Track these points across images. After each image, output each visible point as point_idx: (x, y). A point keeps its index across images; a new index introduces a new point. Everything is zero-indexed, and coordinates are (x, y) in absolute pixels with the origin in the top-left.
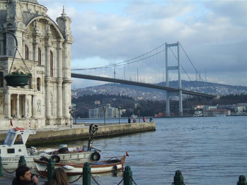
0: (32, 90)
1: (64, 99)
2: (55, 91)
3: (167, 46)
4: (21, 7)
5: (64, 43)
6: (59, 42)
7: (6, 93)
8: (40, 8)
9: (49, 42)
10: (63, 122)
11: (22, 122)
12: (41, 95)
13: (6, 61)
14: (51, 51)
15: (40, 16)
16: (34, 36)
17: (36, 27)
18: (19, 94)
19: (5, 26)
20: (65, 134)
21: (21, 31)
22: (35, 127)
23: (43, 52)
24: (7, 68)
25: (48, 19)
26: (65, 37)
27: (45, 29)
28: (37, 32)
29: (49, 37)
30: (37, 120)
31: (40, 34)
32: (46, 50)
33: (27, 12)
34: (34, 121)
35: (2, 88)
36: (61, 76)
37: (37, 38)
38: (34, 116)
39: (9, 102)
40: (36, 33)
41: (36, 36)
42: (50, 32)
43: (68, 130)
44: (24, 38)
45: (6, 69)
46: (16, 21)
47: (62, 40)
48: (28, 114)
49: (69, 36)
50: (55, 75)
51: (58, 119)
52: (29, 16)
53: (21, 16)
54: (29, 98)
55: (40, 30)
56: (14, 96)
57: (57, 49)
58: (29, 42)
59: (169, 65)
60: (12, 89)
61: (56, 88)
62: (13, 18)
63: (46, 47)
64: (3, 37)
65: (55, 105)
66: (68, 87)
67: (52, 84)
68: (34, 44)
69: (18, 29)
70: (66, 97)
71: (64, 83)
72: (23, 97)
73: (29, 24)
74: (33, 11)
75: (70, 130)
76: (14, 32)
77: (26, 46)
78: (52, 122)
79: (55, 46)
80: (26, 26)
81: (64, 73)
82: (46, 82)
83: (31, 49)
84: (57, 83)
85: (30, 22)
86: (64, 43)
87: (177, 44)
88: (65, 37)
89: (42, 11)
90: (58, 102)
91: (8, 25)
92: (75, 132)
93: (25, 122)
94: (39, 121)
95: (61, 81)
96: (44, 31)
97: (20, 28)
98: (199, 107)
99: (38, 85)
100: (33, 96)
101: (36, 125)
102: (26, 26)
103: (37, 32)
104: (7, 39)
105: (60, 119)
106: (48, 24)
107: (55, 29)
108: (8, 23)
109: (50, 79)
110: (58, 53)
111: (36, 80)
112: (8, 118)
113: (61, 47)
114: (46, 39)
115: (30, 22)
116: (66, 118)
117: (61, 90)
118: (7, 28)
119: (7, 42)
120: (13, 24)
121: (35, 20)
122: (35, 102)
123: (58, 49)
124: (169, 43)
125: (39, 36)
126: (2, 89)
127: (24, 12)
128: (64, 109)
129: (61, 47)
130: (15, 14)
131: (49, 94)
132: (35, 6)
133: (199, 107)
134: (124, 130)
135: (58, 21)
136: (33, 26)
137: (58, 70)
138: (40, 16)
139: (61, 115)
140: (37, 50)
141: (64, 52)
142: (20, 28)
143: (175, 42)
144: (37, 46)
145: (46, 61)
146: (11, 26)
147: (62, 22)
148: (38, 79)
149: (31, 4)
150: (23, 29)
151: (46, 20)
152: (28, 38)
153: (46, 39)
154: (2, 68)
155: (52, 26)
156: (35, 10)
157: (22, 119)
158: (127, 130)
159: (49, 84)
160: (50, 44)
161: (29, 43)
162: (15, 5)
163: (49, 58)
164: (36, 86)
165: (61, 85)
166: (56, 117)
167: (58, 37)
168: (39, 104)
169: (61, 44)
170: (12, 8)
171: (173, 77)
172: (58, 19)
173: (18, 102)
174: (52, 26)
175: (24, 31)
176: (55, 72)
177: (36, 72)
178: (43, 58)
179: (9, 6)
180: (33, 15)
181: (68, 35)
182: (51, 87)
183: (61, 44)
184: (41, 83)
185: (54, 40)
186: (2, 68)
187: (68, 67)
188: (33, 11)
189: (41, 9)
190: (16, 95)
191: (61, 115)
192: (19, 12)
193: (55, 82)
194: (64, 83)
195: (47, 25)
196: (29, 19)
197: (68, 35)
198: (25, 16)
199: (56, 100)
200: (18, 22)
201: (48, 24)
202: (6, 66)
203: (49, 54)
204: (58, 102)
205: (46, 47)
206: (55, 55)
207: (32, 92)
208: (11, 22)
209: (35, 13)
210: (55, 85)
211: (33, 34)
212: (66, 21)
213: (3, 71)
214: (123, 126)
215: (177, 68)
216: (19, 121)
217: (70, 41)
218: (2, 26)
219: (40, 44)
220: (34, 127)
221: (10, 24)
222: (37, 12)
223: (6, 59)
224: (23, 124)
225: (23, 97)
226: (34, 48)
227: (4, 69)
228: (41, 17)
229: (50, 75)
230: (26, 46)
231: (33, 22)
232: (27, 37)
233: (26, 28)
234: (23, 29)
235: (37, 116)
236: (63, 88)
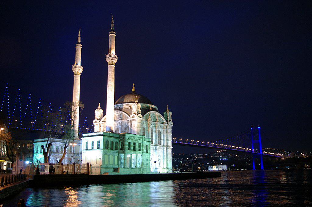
2: (162, 153)
14: (159, 131)
50: (162, 144)
164: (145, 150)
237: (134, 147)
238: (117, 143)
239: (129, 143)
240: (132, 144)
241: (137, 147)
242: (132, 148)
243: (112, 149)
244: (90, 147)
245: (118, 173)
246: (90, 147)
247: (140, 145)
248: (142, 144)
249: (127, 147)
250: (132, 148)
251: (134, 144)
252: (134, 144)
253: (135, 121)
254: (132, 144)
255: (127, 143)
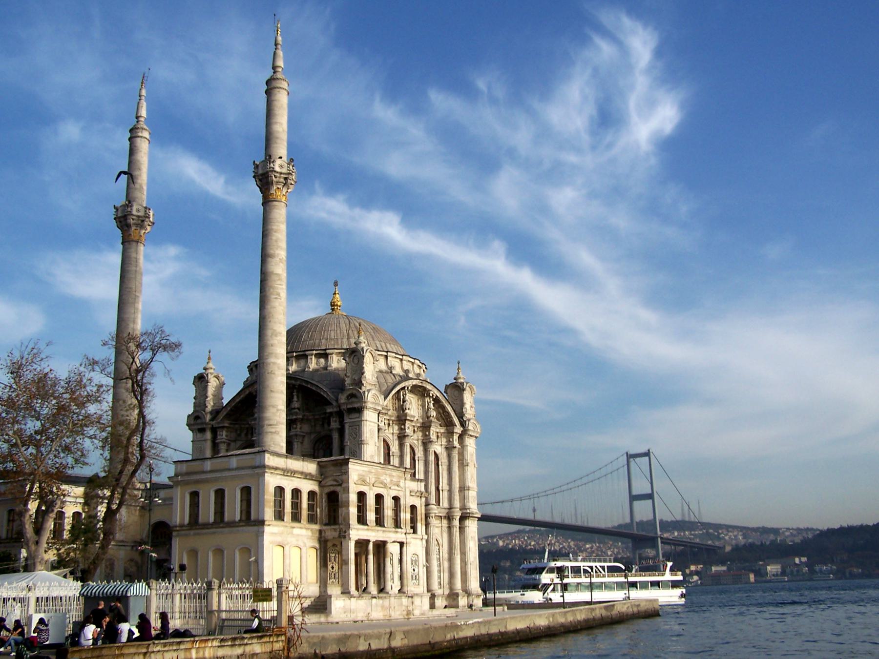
0: (400, 530)
1: (463, 553)
2: (445, 535)
3: (630, 457)
4: (375, 360)
5: (461, 437)
6: (450, 433)
7: (345, 537)
8: (413, 364)
9: (431, 432)
10: (463, 601)
11: (381, 601)
12: (419, 542)
13: (344, 467)
15: (412, 379)
16: (401, 419)
17: (404, 401)
18: (373, 539)
19: (343, 399)
20: (484, 631)
21: (376, 410)
22: (408, 614)
23: (420, 453)
24: (348, 482)
25: (429, 387)
26: (463, 424)
27: (423, 406)
28: (407, 411)
29: (431, 422)
30: (412, 597)
31: (414, 417)
32: (426, 451)
33: (386, 372)
34: (405, 601)
35: (336, 527)
36: (457, 504)
37: (408, 424)
38: (405, 589)
39: (352, 556)
40: (406, 415)
41: (406, 420)
42: (433, 413)
43: (488, 623)
44: (382, 425)
45: (344, 485)
46: (363, 389)
47: (458, 429)
48: (393, 585)
49: (472, 421)
51: (453, 596)
52: (390, 380)
53: (375, 379)
54: (393, 549)
55: (414, 408)
56: (362, 545)
57: (447, 448)
58: (391, 433)
59: (634, 493)
60: (358, 529)
61: (445, 529)
62: (359, 384)
63: (426, 443)
64: (338, 423)
65: (446, 564)
66: (472, 527)
67: (439, 521)
68: (402, 437)
69: (369, 405)
70: (467, 549)
71: (463, 518)
72: (381, 547)
73: (391, 395)
74: (398, 370)
75: (495, 620)
76: (359, 411)
77: (384, 440)
78: (440, 602)
79: (444, 441)
80: (385, 398)
81: (463, 499)
82: (427, 516)
83: (395, 448)
84: (449, 518)
85: (394, 392)
86: (461, 437)
87: (647, 454)
88: (463, 424)
89: (417, 370)
90: (451, 559)
91: (347, 397)
92: (506, 627)
93: (386, 602)
94: (417, 600)
95: (457, 514)
96: (421, 411)
97: (373, 403)
98: (693, 568)
99: (413, 521)
100: (402, 544)
101: (410, 608)
102: (385, 398)
103: (407, 411)
104: (347, 427)
105: (457, 595)
106: (428, 395)
107: (443, 407)
108: (349, 393)
109: (435, 510)
110: (449, 456)
111: (408, 510)
112: (349, 593)
113: (456, 444)
114: (425, 427)
115: (394, 392)
116: (468, 593)
117: (458, 533)
118: (347, 404)
119: (347, 431)
120: (358, 394)
121: (403, 388)
122: (407, 558)
123: (449, 448)
124: (632, 451)
125: (412, 421)
126: (335, 530)
127: (381, 371)
128: (464, 574)
129: (456, 444)
130: (363, 373)
131: (433, 544)
132: (401, 360)
133: (693, 568)
134: (602, 618)
135: (449, 391)
136: (399, 400)
137: (450, 492)
138: (412, 379)
139: (458, 585)
140: (407, 450)
141: (461, 454)
142: (373, 403)
143: (643, 450)
144: (408, 442)
145: (426, 472)
146: (353, 399)
147: (456, 392)
148: (413, 508)
149: (394, 355)
150: (379, 404)
151: (425, 389)
152: (389, 425)
153: (425, 427)
154: (335, 483)
155: (437, 401)
156: (402, 367)
157: (380, 595)
158: (608, 617)
159: (434, 522)
160: (433, 437)
161: (391, 436)
162: (363, 356)
163: (432, 467)
165: (456, 523)
166: (447, 592)
167: (448, 424)
168: (415, 562)
169: (456, 437)
170: (356, 361)
171: (643, 512)
172: (447, 387)
173: (371, 557)
174: (437, 401)
175: (380, 408)
176: (444, 496)
177: (408, 493)
178: (420, 466)
179: (349, 357)
180: (398, 378)
181: (469, 420)
182: (438, 528)
183: (456, 437)
184: (419, 518)
185: (442, 431)
186: (335, 483)
187: (470, 485)
188: (398, 370)
189: (415, 366)
190: (368, 541)
191: (458, 585)
192: (371, 368)
193: (445, 517)
194: (463, 518)
195: (427, 399)
196: (391, 386)
197: (469, 420)
198: (382, 380)
199: (446, 556)
200: (369, 391)
201: (428, 395)
202: (344, 477)
203: (432, 458)
204: (451, 559)
205: (426, 443)
206: (443, 460)
207: (401, 537)
208: (354, 392)
209: (402, 373)
210: (445, 523)
211: (398, 417)
212: (464, 390)
213: (338, 489)
214: (601, 608)
215: (650, 496)
216: (374, 600)
217: (474, 431)
218: (337, 401)
219: (414, 439)
220: (405, 613)
221: (352, 396)
222: (407, 372)
223: (346, 462)
224: (383, 607)
225: (381, 547)
226: (401, 446)
227: (340, 485)
228: (415, 382)
229: (434, 502)
230: (384, 440)
231: (399, 392)
232: (387, 422)
233: (385, 403)
234: (379, 404)
235: (411, 588)
236: (462, 529)
237: (379, 511)
238: (311, 494)
239: (361, 496)
240: (371, 501)
241: (388, 512)
242: (371, 516)
243: (296, 517)
244: (208, 513)
245: (327, 616)
246: (208, 513)
247: (396, 499)
248: (402, 502)
249: (353, 511)
250: (371, 516)
251: (379, 498)
252: (379, 498)
253: (357, 415)
254: (371, 501)
255: (353, 498)
